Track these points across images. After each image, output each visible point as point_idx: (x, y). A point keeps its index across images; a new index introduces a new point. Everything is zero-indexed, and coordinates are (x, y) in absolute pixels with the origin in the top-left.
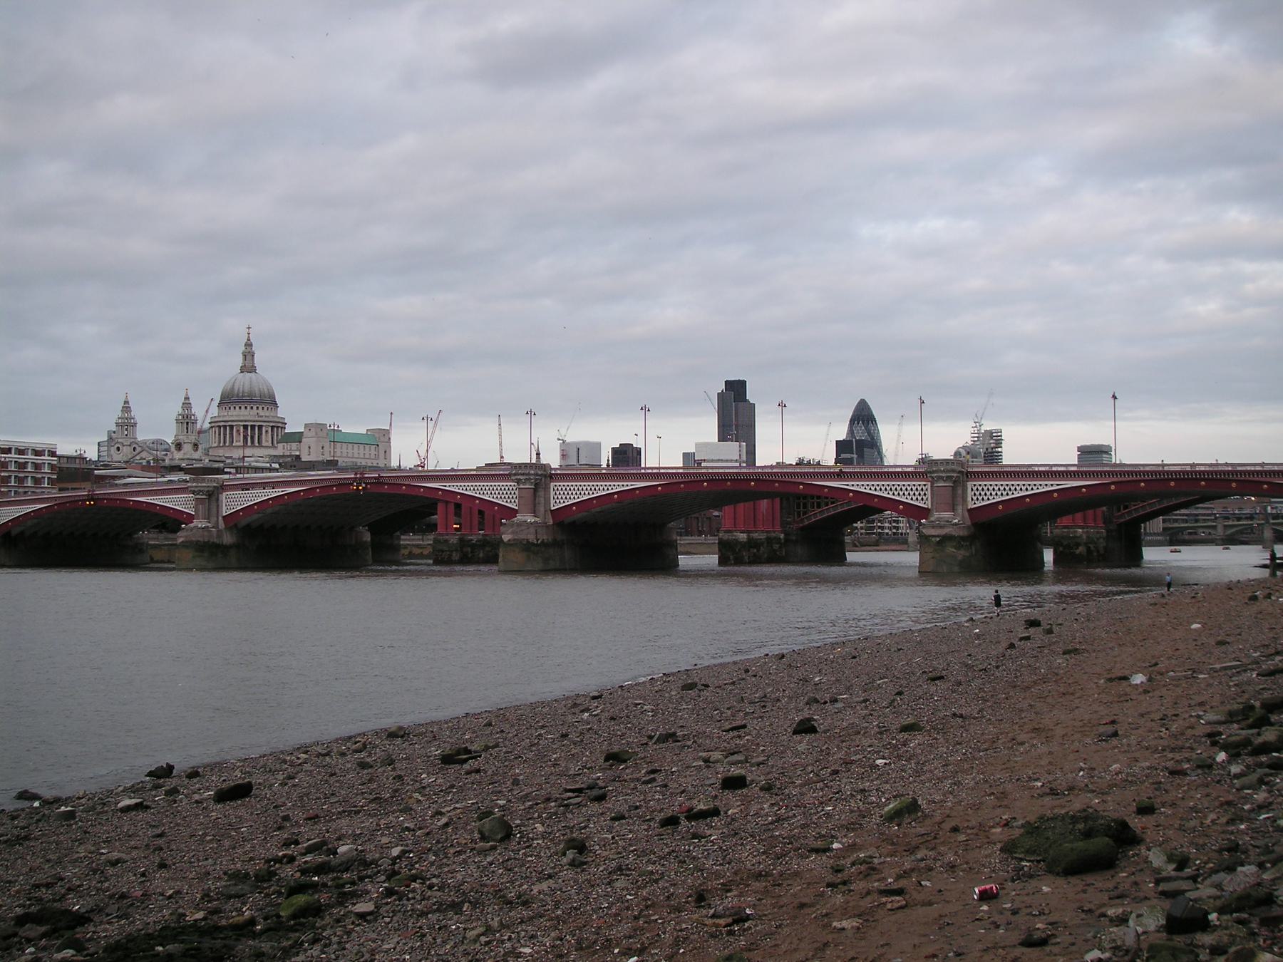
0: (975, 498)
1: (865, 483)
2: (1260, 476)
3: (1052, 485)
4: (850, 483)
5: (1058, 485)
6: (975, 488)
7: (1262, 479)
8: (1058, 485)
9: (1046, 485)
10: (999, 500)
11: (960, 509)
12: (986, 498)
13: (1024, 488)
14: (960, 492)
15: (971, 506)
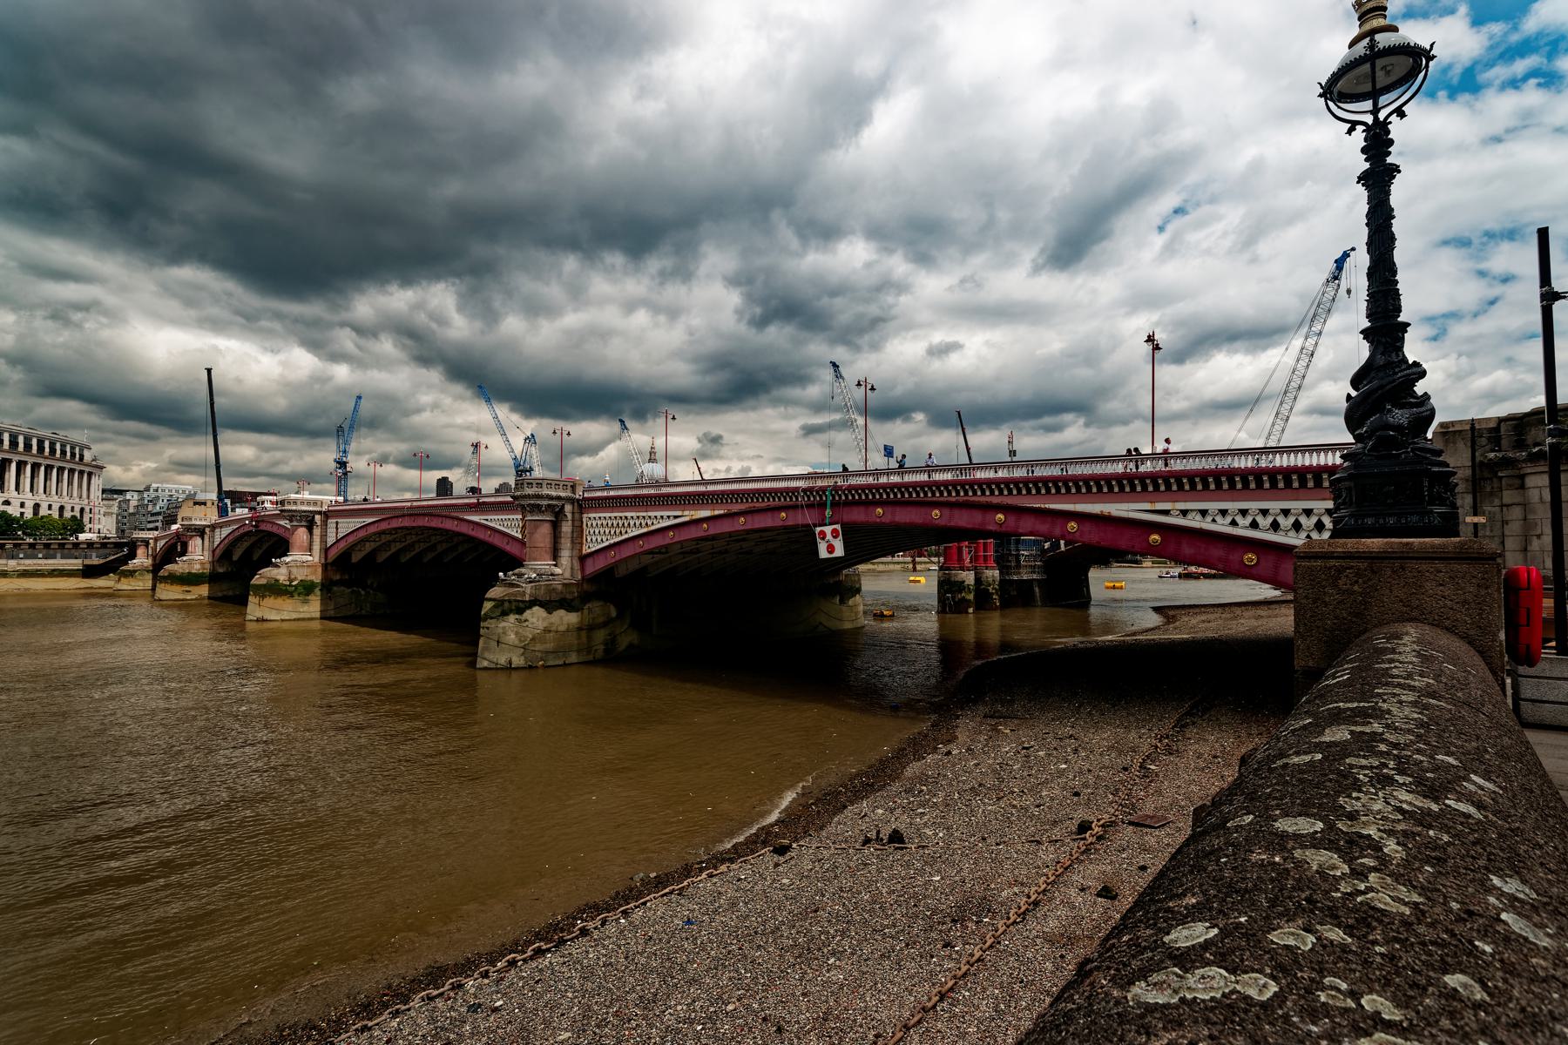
0: (589, 540)
1: (500, 517)
2: (988, 493)
3: (669, 517)
4: (489, 517)
5: (676, 517)
6: (589, 524)
7: (995, 500)
8: (676, 517)
9: (662, 517)
10: (612, 542)
11: (565, 554)
12: (599, 540)
13: (638, 523)
14: (566, 528)
15: (586, 550)
